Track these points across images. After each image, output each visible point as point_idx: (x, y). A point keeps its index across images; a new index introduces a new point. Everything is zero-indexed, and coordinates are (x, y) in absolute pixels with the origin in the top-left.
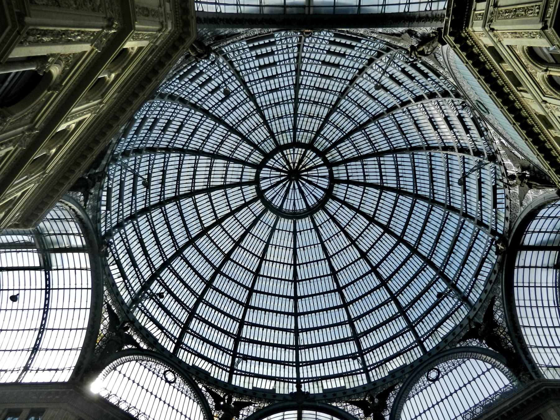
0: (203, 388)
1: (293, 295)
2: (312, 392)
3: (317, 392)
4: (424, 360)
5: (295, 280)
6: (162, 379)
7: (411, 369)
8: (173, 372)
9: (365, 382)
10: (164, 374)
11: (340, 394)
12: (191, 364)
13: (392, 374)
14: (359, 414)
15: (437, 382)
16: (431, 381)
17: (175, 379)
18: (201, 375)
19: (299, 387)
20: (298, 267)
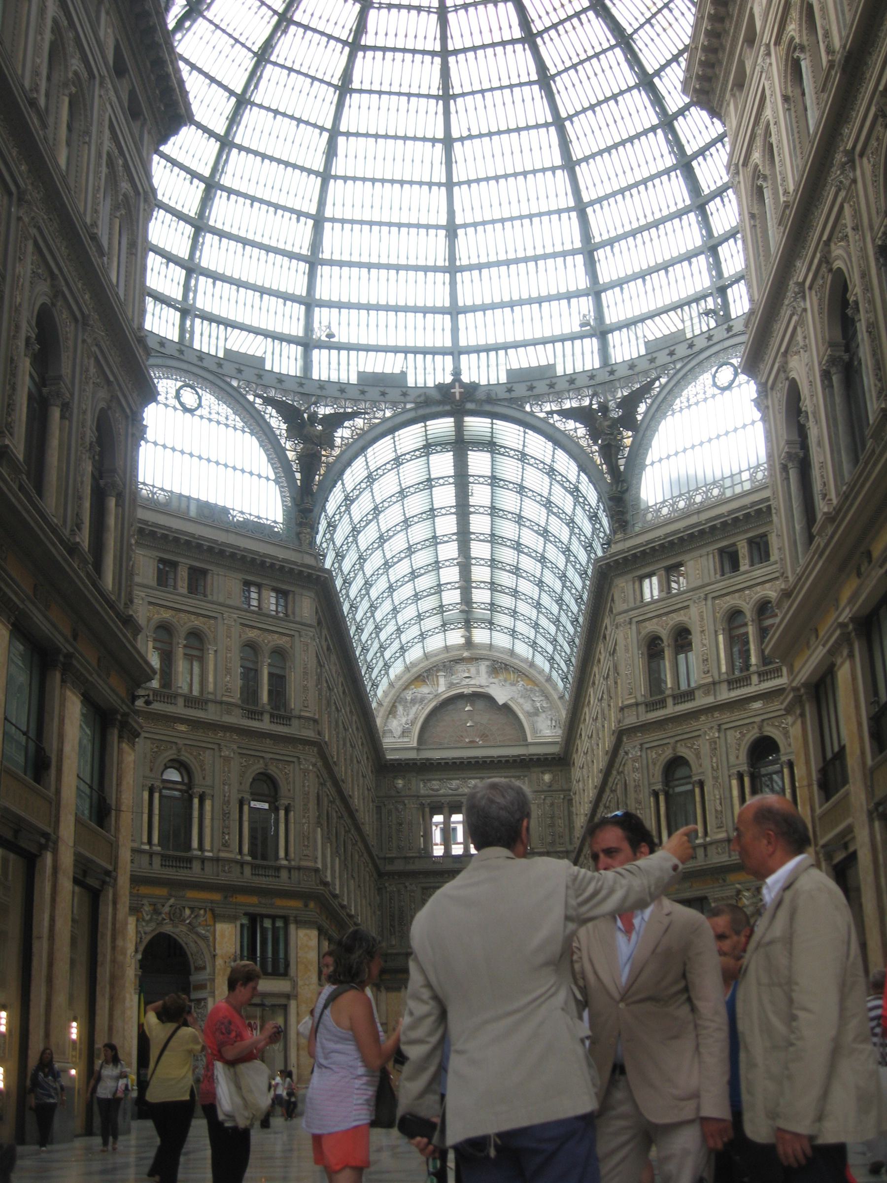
0: (258, 401)
1: (440, 135)
2: (484, 382)
3: (493, 381)
4: (715, 340)
5: (446, 96)
6: (175, 408)
7: (690, 352)
8: (193, 388)
9: (597, 365)
10: (178, 396)
11: (541, 387)
12: (221, 354)
13: (653, 348)
14: (576, 429)
15: (727, 393)
16: (718, 388)
17: (200, 398)
18: (249, 374)
19: (457, 373)
20: (452, 60)
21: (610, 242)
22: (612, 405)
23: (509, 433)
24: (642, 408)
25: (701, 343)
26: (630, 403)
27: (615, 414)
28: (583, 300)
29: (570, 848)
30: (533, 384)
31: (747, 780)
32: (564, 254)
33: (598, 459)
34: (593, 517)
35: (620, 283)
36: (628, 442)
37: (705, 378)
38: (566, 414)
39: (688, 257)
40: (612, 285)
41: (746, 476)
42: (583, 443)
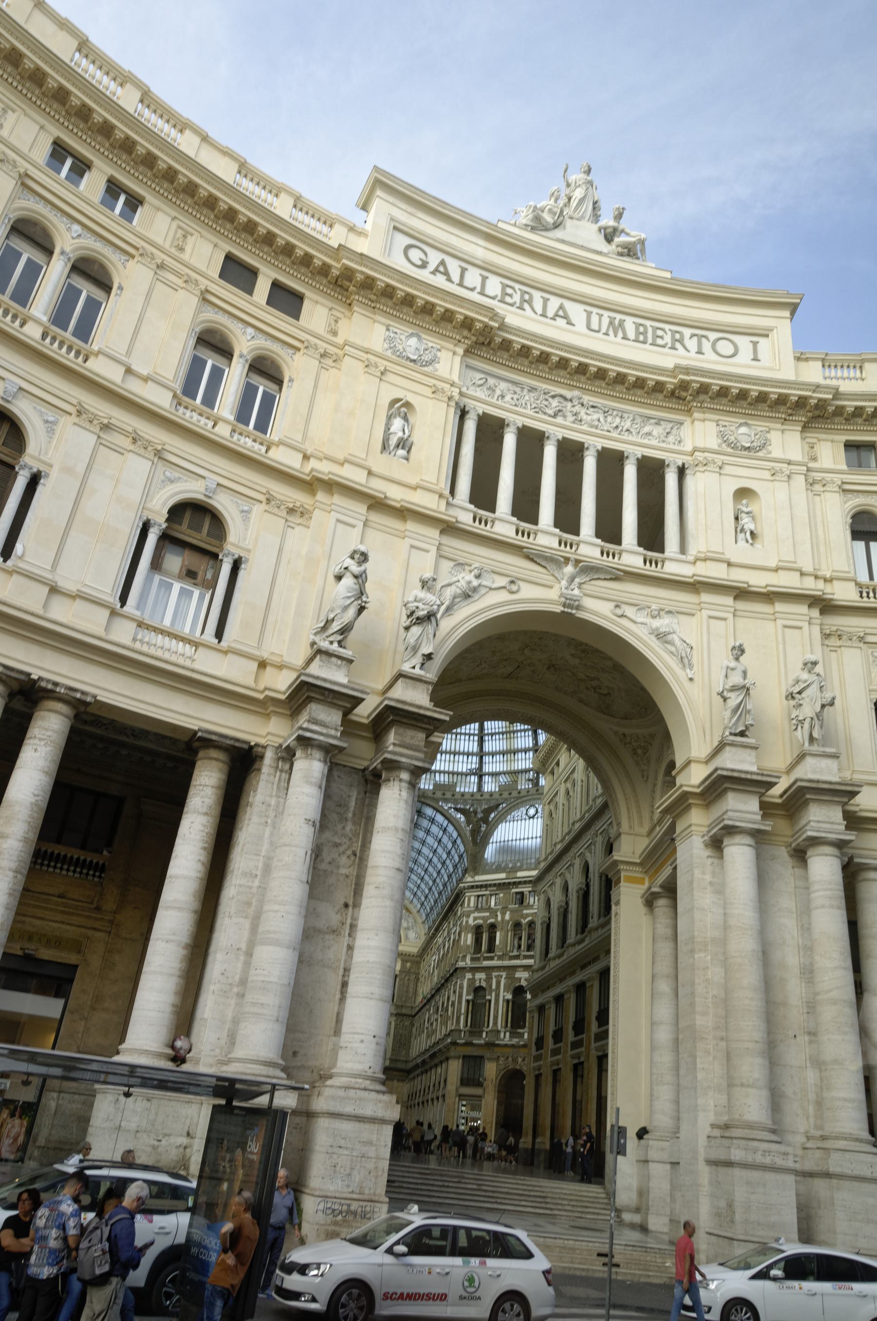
3: (427, 787)
9: (475, 790)
11: (448, 795)
21: (492, 735)
22: (479, 810)
23: (429, 811)
24: (492, 815)
25: (523, 793)
26: (487, 812)
27: (480, 815)
28: (474, 758)
29: (414, 1006)
30: (445, 791)
31: (510, 1004)
32: (470, 735)
33: (468, 834)
34: (461, 857)
35: (493, 754)
36: (483, 829)
37: (523, 810)
38: (456, 809)
39: (526, 751)
40: (489, 754)
41: (533, 861)
42: (463, 825)
